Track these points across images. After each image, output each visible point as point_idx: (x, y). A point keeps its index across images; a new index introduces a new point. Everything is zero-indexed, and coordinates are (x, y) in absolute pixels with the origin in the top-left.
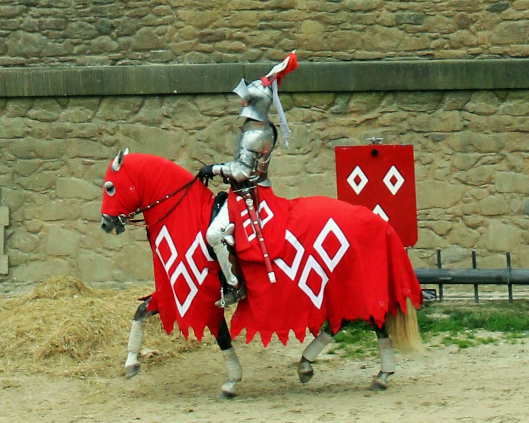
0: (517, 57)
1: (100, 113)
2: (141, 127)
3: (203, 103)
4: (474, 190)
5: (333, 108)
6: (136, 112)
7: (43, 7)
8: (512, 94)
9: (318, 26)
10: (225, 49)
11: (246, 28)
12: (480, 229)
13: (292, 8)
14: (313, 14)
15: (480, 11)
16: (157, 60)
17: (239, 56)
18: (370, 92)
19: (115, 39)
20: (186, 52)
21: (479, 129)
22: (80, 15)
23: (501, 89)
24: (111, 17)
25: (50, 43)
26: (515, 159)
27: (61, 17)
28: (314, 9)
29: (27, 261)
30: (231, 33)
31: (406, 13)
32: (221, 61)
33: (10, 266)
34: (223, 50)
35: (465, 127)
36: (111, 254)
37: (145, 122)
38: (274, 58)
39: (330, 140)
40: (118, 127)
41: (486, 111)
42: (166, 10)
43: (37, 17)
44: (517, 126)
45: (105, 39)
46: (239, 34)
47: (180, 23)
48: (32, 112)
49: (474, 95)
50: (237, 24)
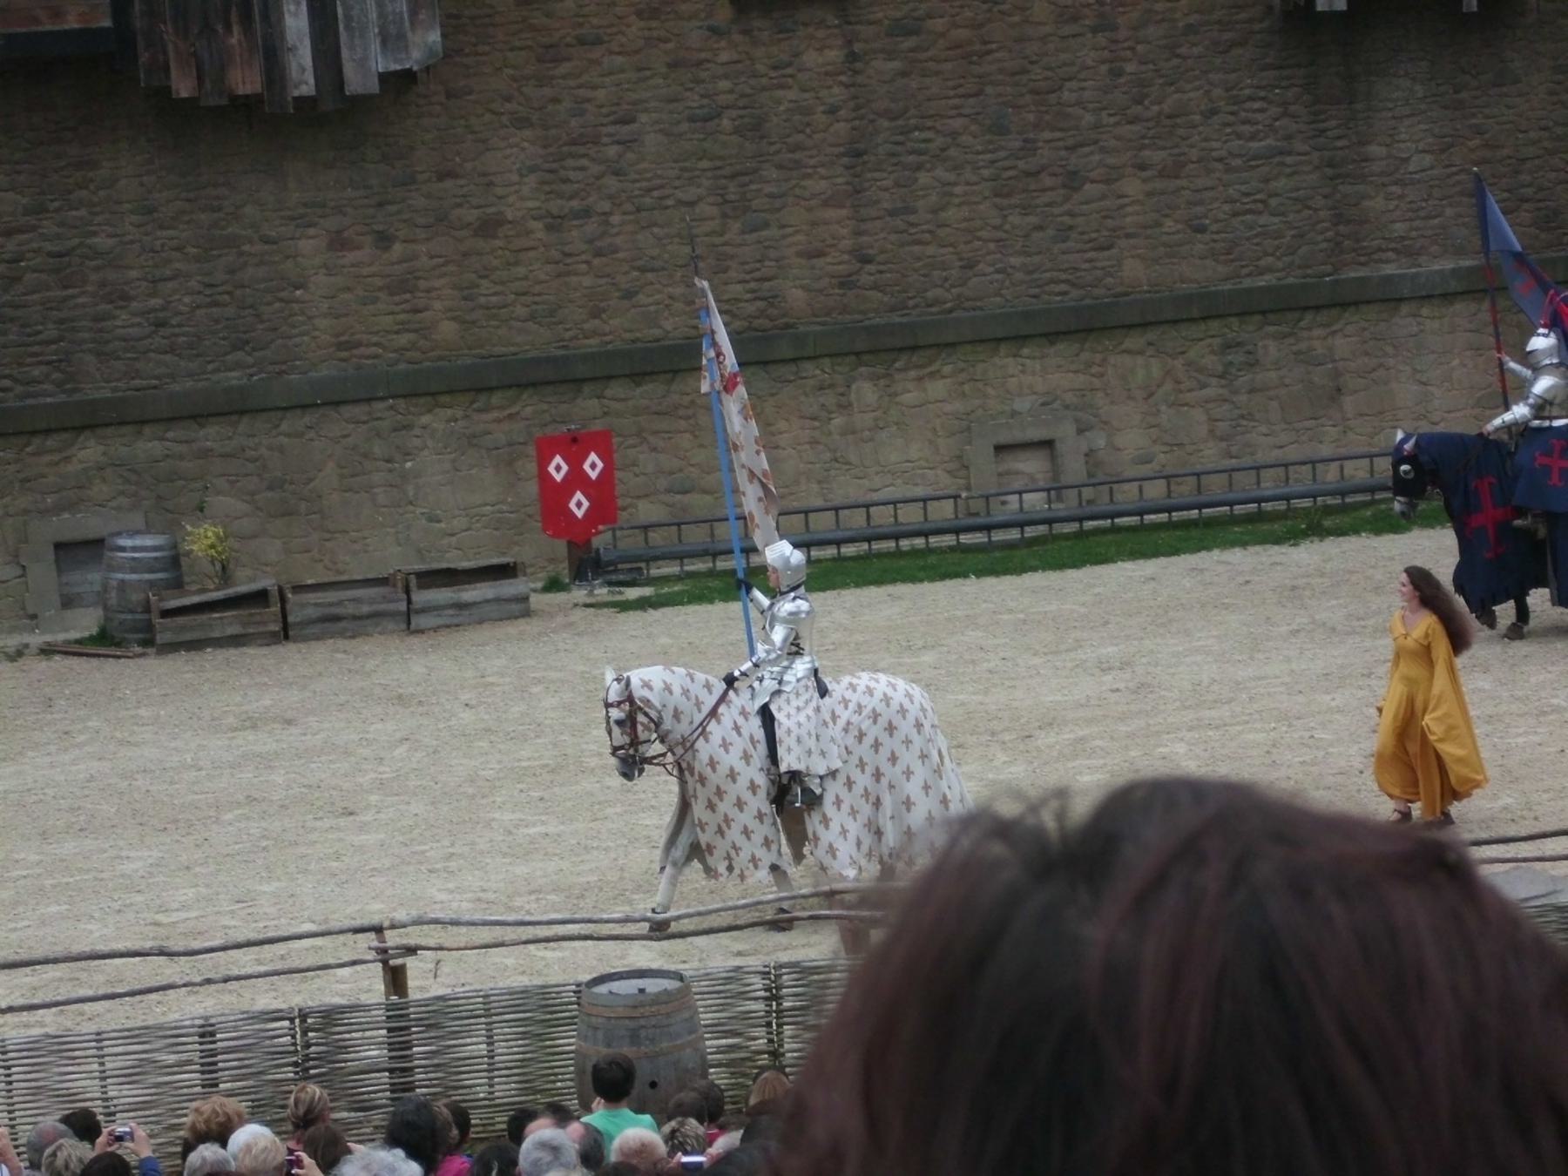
2: (285, 440)
3: (348, 411)
5: (475, 406)
6: (278, 426)
8: (647, 378)
12: (629, 510)
14: (449, 314)
18: (510, 387)
19: (250, 355)
23: (637, 375)
24: (245, 332)
25: (183, 363)
31: (539, 307)
35: (605, 413)
36: (268, 569)
37: (288, 435)
41: (623, 396)
45: (239, 355)
46: (375, 339)
47: (317, 333)
48: (170, 435)
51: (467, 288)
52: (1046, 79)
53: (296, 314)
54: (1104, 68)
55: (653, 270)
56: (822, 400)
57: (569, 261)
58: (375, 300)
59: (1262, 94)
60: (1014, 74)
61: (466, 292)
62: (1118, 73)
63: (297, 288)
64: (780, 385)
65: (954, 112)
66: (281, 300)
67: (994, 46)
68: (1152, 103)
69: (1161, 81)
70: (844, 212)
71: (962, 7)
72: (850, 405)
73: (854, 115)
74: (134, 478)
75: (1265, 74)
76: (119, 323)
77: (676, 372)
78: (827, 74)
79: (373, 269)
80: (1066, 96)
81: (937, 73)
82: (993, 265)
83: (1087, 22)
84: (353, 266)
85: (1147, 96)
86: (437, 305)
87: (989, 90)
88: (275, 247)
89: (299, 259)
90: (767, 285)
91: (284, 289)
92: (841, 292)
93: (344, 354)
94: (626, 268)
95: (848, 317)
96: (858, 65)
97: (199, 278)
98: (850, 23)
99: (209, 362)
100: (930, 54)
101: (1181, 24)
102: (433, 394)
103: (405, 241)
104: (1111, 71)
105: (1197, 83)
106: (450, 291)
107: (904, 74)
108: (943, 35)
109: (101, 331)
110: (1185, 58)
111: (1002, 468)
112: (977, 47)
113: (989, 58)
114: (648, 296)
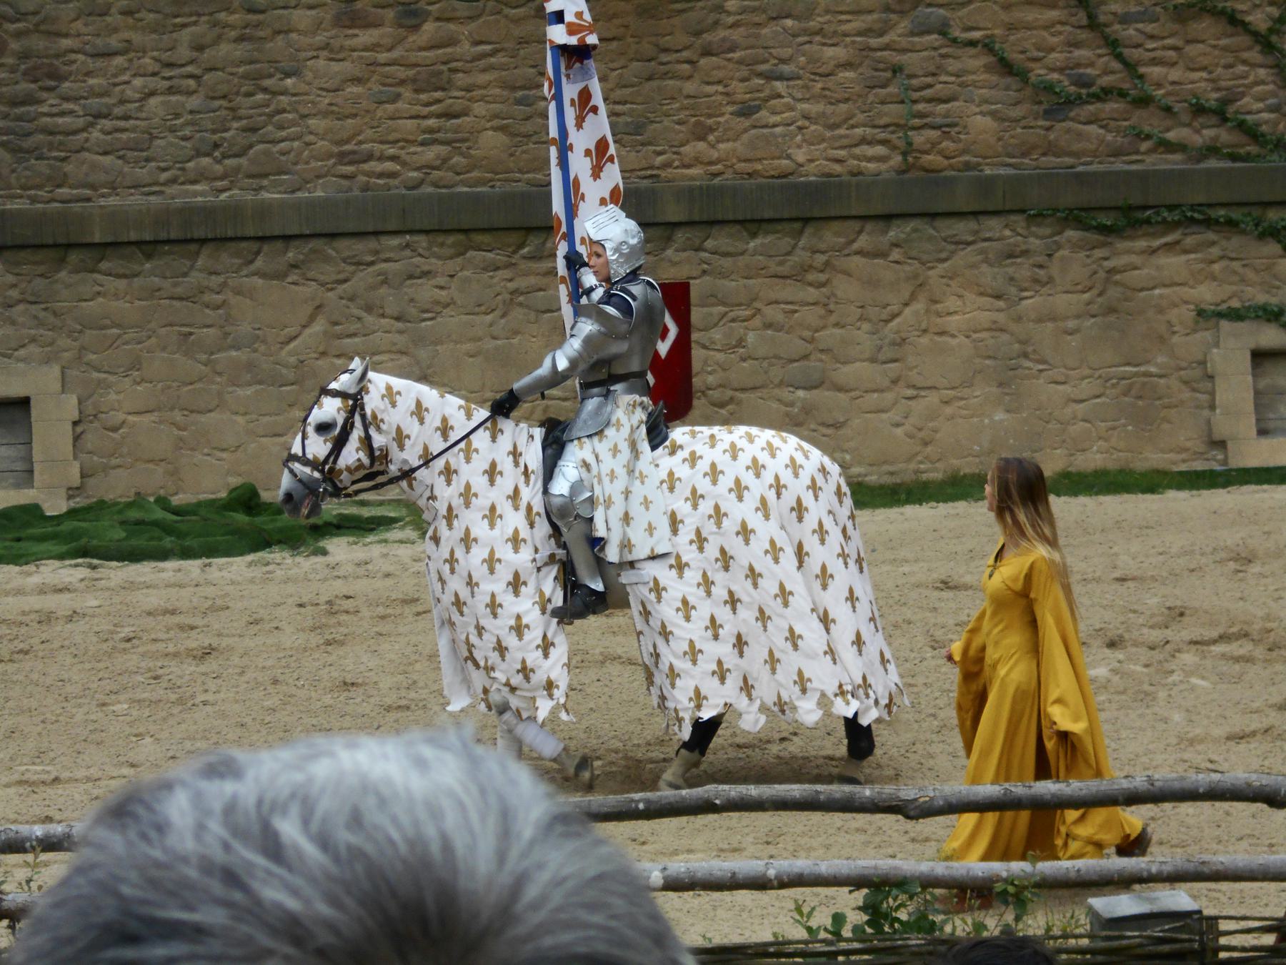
0: (773, 177)
1: (200, 263)
2: (258, 282)
3: (347, 247)
4: (720, 357)
6: (251, 262)
7: (118, 118)
8: (764, 226)
9: (502, 138)
10: (373, 172)
11: (401, 144)
12: (730, 407)
13: (466, 115)
14: (496, 122)
15: (722, 115)
16: (282, 189)
17: (396, 182)
19: (219, 162)
20: (318, 177)
21: (724, 275)
22: (173, 130)
24: (214, 132)
26: (773, 313)
27: (143, 132)
28: (496, 116)
29: (106, 469)
30: (382, 151)
32: (367, 190)
33: (83, 476)
34: (369, 174)
35: (704, 272)
36: (224, 455)
38: (441, 184)
39: (522, 294)
40: (225, 284)
41: (731, 249)
42: (293, 120)
43: (109, 133)
44: (774, 268)
45: (205, 161)
46: (391, 151)
47: (311, 138)
48: (104, 265)
49: (715, 230)
50: (390, 138)
51: (523, 88)
53: (284, 111)
55: (781, 78)
56: (1010, 270)
57: (664, 58)
58: (398, 97)
61: (520, 94)
63: (288, 75)
64: (953, 247)
66: (265, 90)
70: (1054, 14)
72: (1050, 280)
74: (52, 319)
76: (45, 109)
77: (806, 221)
79: (395, 54)
82: (1261, 100)
84: (366, 49)
86: (479, 108)
88: (261, 17)
89: (294, 36)
90: (942, 108)
91: (271, 76)
92: (1047, 124)
93: (350, 169)
94: (744, 72)
95: (1051, 160)
97: (155, 54)
99: (164, 170)
102: (466, 231)
103: (438, 19)
106: (497, 91)
109: (19, 118)
111: (1263, 383)
114: (774, 113)
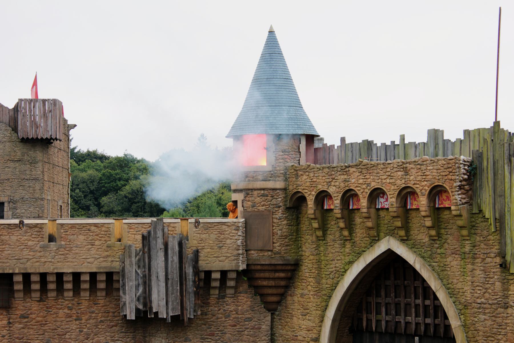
52: (62, 332)
54: (78, 330)
59: (121, 339)
60: (53, 330)
62: (82, 331)
65: (36, 339)
67: (48, 322)
68: (90, 340)
69: (93, 334)
71: (40, 312)
73: (9, 338)
75: (122, 334)
78: (2, 327)
80: (67, 336)
81: (32, 328)
83: (74, 318)
85: (89, 338)
87: (46, 334)
96: (11, 325)
98: (9, 314)
100: (30, 323)
101: (99, 320)
104: (80, 330)
105: (103, 335)
107: (23, 328)
108: (34, 319)
110: (100, 329)
112: (44, 322)
113: (47, 325)
